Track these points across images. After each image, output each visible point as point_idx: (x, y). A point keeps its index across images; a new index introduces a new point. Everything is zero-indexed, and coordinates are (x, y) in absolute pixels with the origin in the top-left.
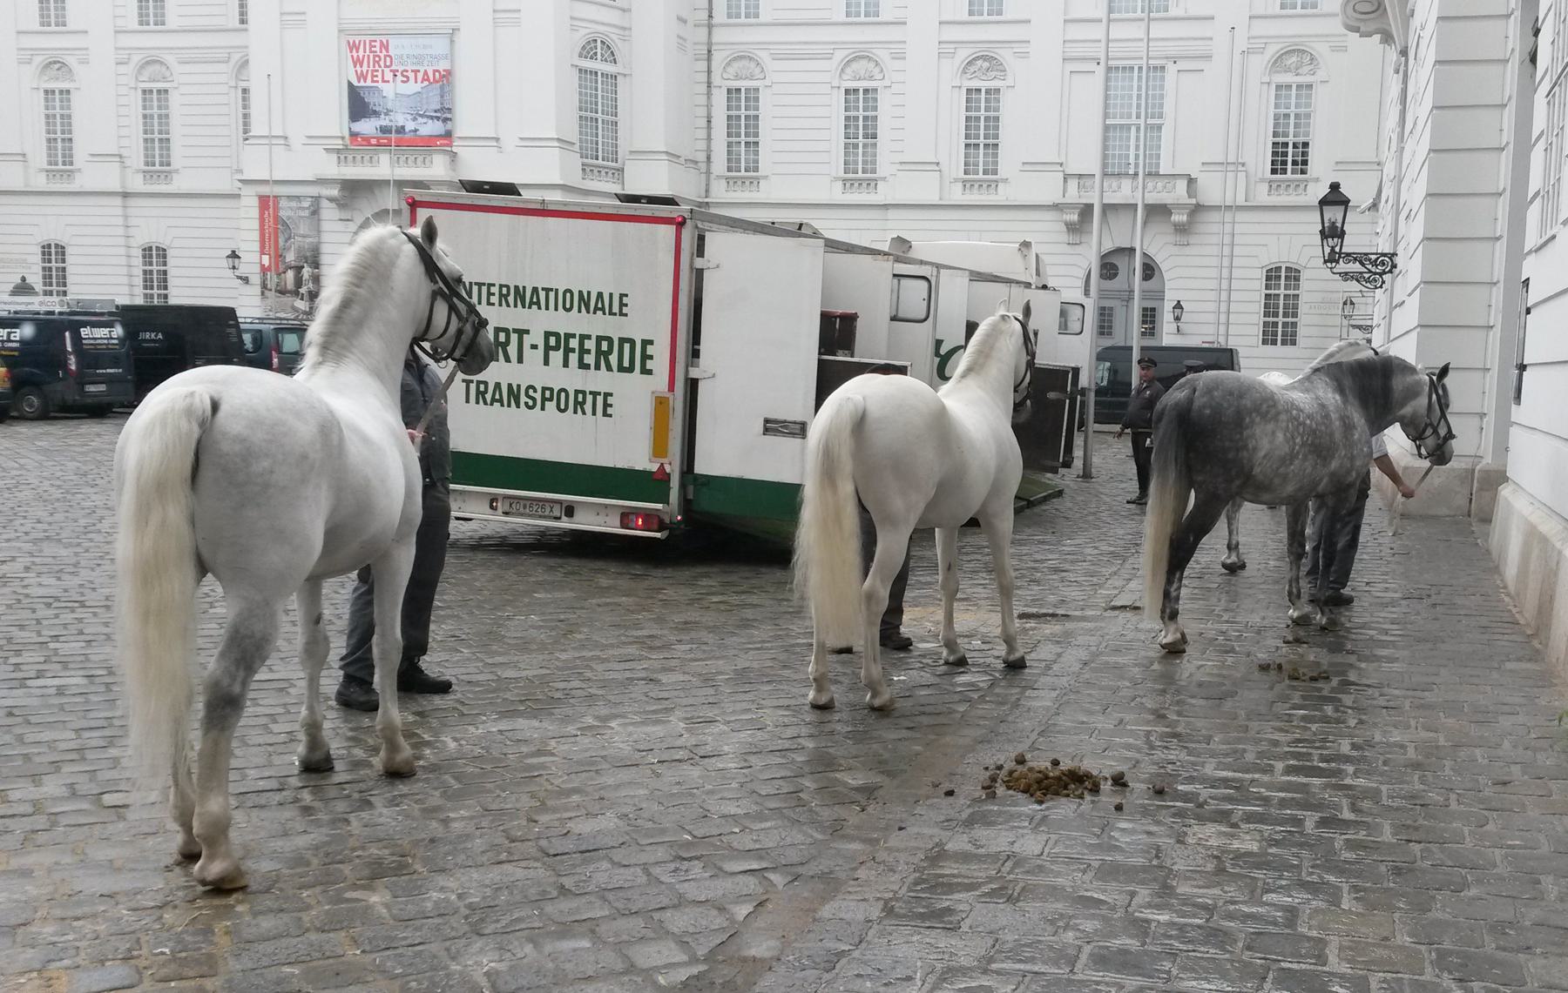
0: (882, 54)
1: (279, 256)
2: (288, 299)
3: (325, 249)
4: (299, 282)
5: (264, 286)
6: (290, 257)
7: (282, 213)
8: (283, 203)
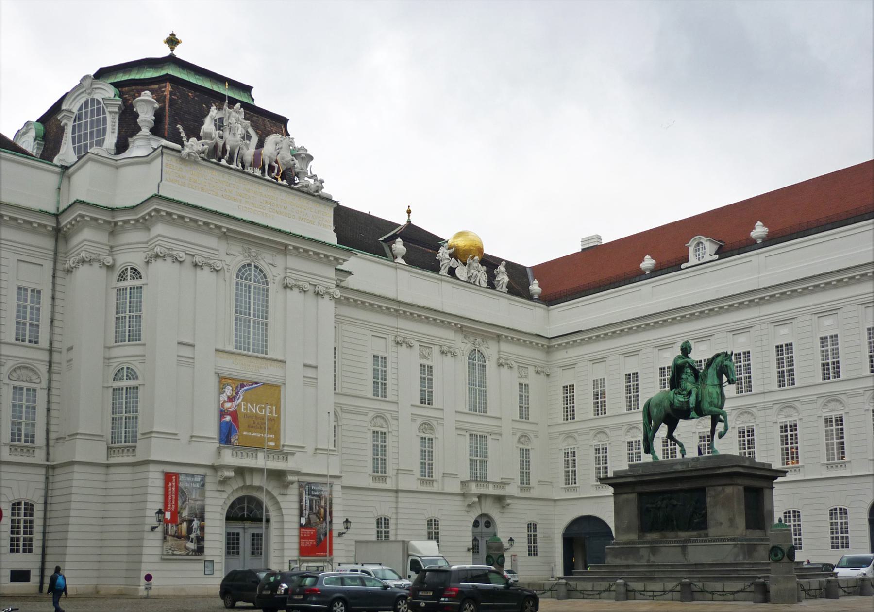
0: (389, 416)
1: (175, 514)
2: (182, 542)
3: (206, 510)
4: (190, 530)
5: (166, 533)
6: (185, 514)
7: (180, 485)
8: (182, 478)
